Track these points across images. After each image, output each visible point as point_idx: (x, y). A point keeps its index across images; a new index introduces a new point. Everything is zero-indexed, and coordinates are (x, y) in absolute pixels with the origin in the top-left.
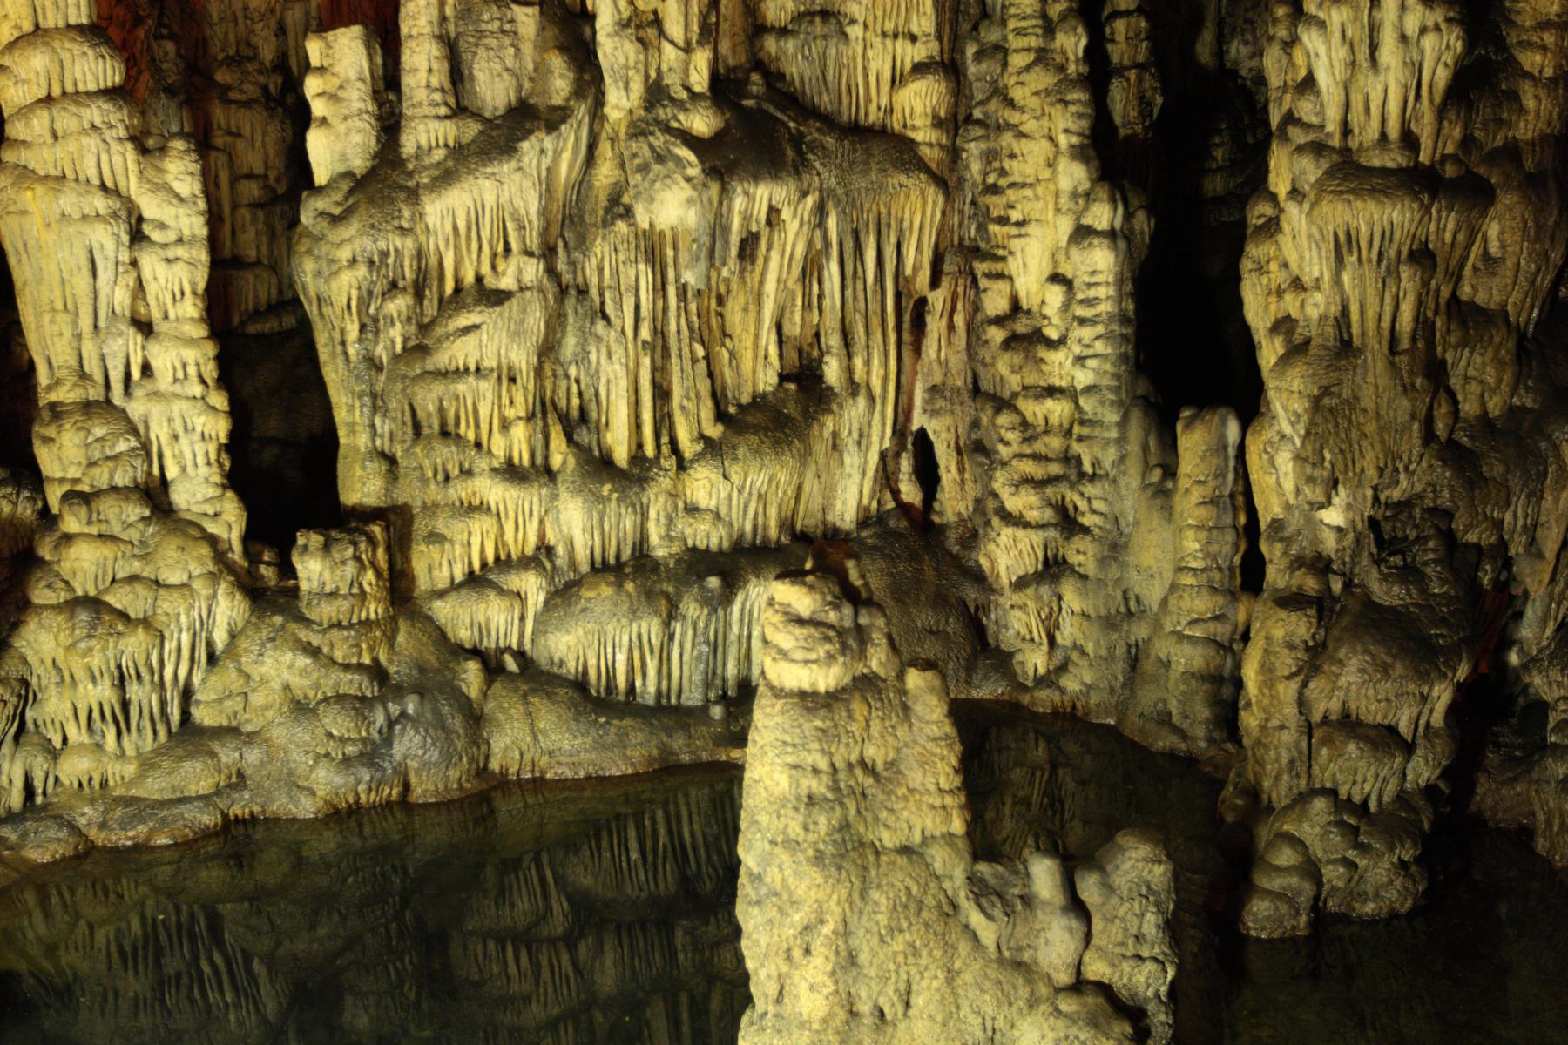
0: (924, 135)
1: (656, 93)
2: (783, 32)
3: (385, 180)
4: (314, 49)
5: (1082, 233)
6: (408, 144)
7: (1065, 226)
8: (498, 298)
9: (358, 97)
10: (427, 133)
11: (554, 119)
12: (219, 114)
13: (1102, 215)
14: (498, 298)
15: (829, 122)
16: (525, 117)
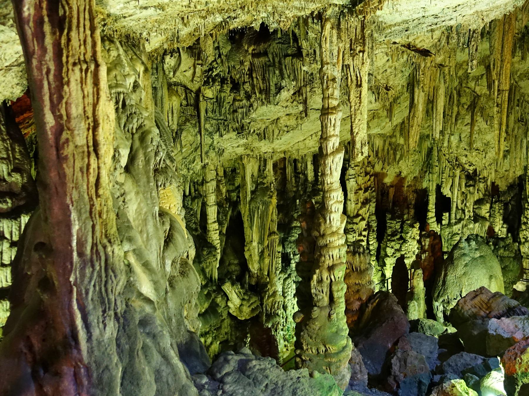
0: (488, 218)
1: (470, 217)
2: (476, 209)
3: (450, 225)
4: (444, 214)
5: (502, 227)
6: (452, 222)
7: (501, 226)
8: (459, 234)
9: (448, 218)
10: (453, 221)
11: (463, 219)
12: (410, 210)
13: (505, 226)
14: (459, 234)
15: (479, 216)
16: (460, 220)
